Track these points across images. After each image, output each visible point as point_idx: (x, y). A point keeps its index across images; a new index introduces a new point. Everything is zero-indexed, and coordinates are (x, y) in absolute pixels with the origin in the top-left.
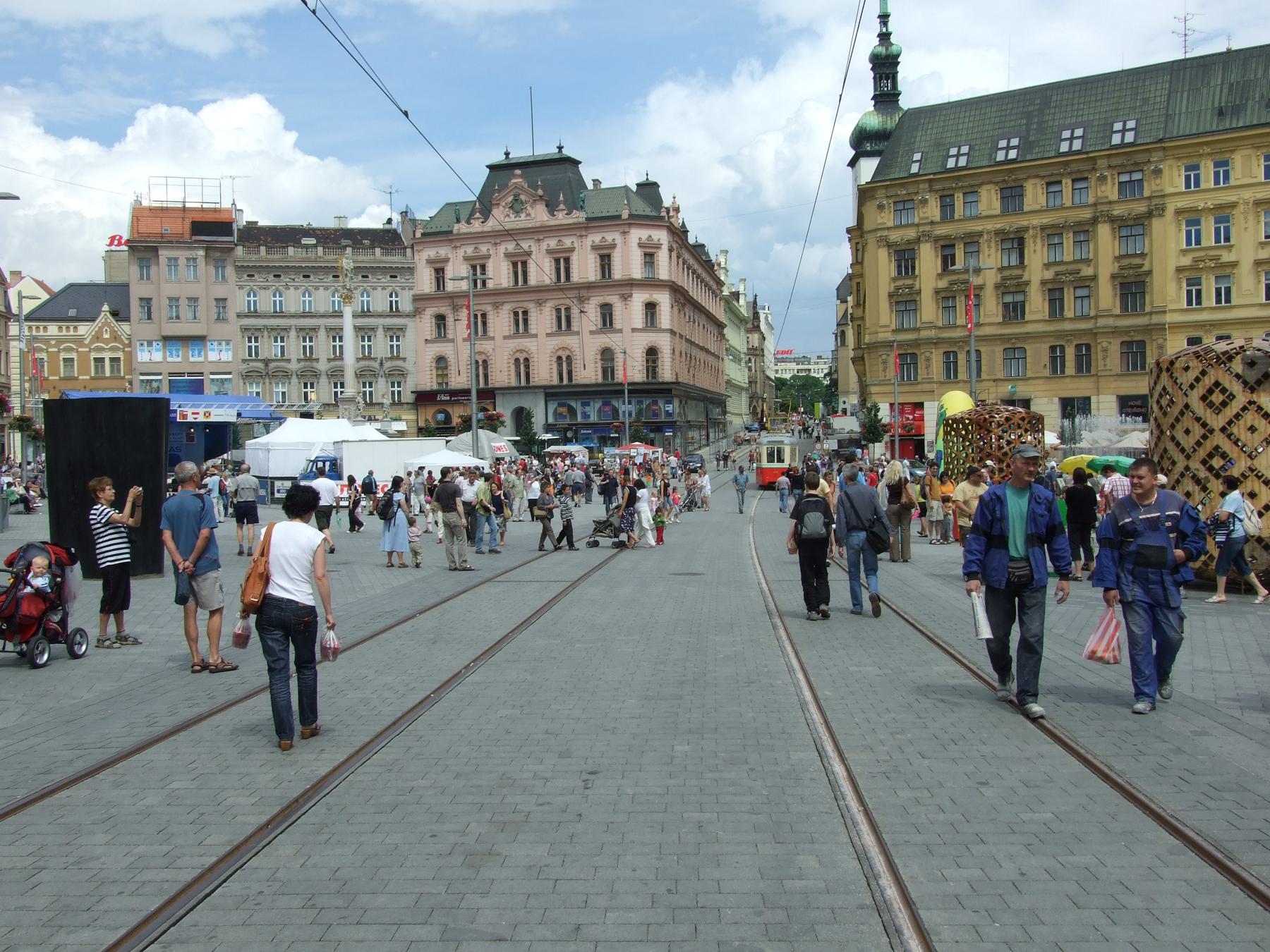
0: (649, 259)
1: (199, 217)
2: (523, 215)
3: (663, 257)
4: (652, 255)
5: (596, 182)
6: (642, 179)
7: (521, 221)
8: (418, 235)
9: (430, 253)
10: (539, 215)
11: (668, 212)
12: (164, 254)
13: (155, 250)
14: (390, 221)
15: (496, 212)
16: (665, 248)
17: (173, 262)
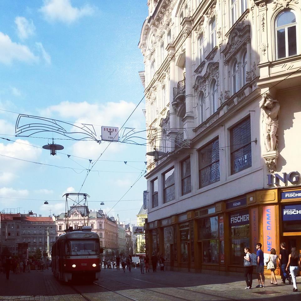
0: (101, 225)
1: (15, 216)
2: (77, 216)
3: (103, 225)
4: (101, 225)
5: (91, 211)
6: (99, 210)
7: (77, 218)
8: (56, 219)
9: (59, 223)
10: (80, 217)
11: (104, 216)
12: (8, 223)
13: (6, 223)
14: (50, 216)
15: (72, 216)
16: (104, 223)
17: (9, 225)
